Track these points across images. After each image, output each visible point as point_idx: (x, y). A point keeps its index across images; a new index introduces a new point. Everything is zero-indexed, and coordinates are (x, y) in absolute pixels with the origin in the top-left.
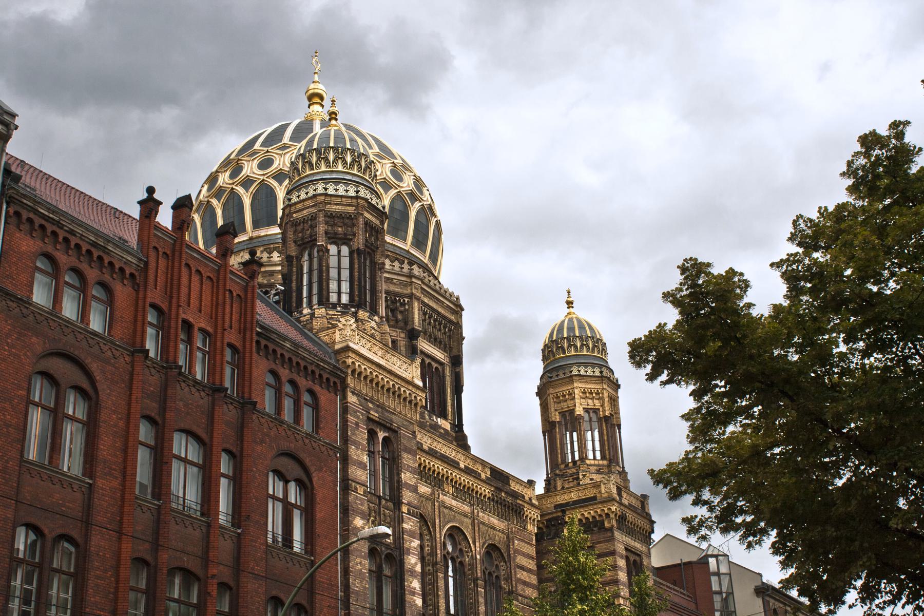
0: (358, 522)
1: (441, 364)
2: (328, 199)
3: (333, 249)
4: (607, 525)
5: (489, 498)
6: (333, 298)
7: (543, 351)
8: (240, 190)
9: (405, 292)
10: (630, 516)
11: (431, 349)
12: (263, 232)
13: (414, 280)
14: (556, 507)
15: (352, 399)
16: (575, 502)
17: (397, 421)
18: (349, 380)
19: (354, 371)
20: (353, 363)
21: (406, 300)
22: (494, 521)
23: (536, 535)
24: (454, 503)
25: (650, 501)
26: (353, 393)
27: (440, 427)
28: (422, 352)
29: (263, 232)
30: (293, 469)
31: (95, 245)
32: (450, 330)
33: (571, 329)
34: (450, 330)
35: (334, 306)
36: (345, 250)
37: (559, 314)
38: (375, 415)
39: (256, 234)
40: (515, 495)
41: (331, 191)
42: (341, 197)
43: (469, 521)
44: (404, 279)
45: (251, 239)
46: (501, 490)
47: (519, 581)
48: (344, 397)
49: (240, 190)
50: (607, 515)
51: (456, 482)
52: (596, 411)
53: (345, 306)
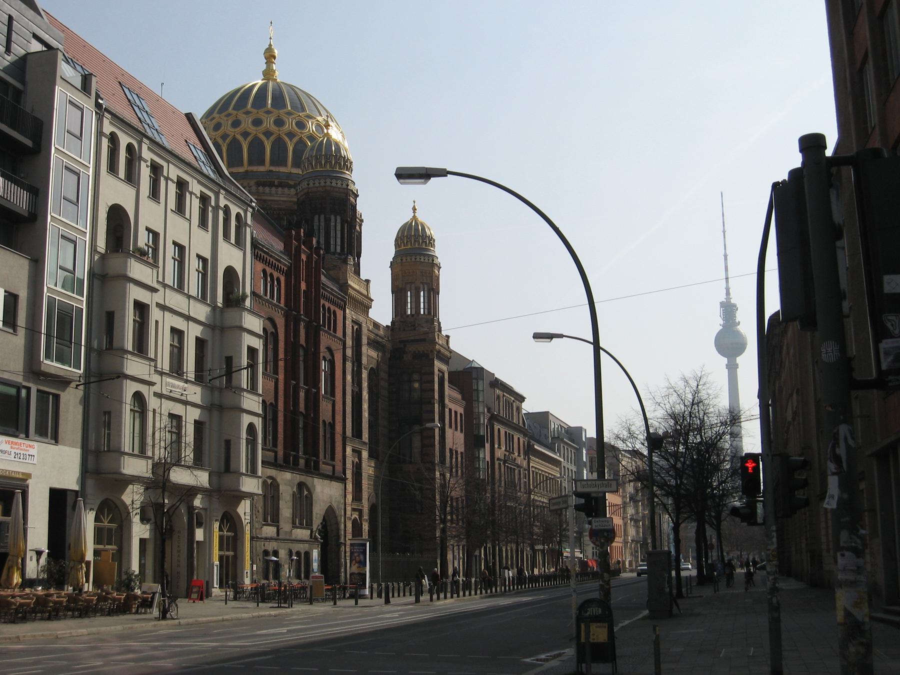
3: (333, 217)
4: (431, 357)
6: (332, 249)
7: (396, 240)
8: (241, 139)
10: (442, 350)
12: (255, 168)
14: (400, 342)
16: (413, 341)
25: (451, 340)
29: (255, 168)
30: (328, 357)
31: (277, 260)
33: (417, 229)
35: (334, 254)
36: (339, 218)
37: (407, 217)
39: (250, 168)
41: (334, 184)
45: (247, 172)
48: (345, 311)
49: (241, 139)
50: (432, 351)
52: (427, 283)
53: (339, 254)
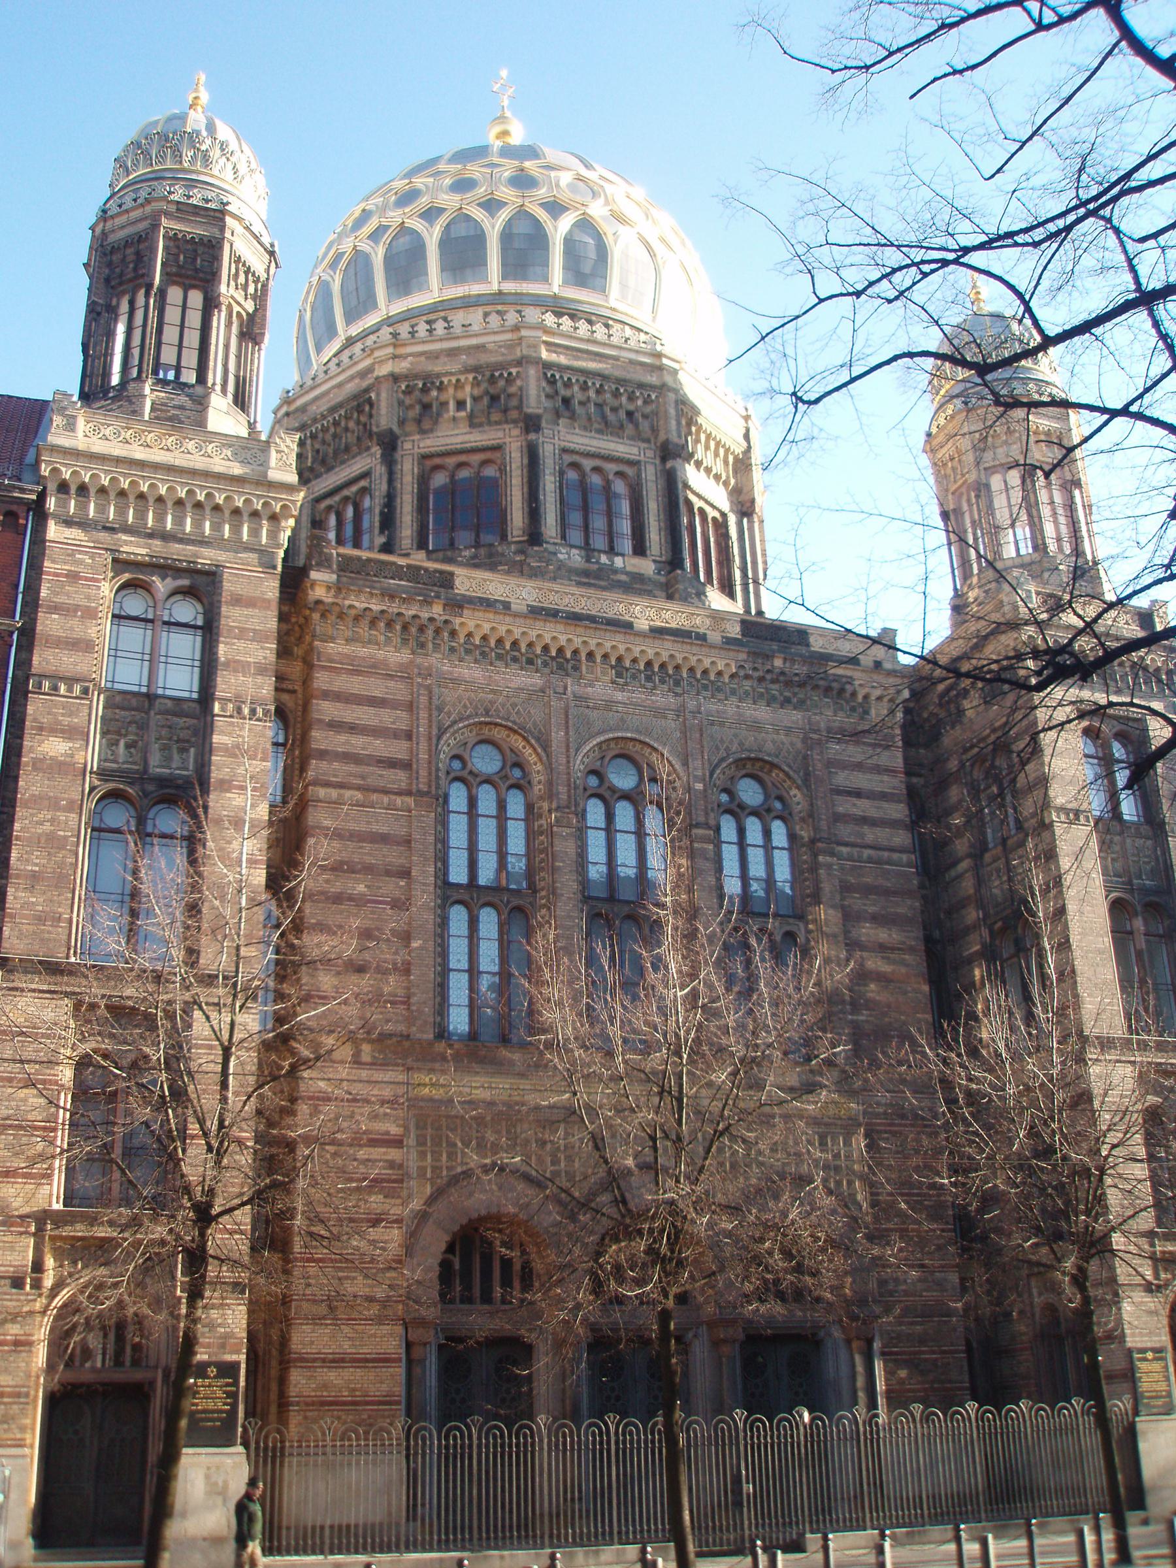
0: (55, 747)
1: (631, 463)
2: (109, 224)
5: (732, 676)
9: (509, 358)
11: (595, 443)
13: (524, 333)
15: (53, 531)
17: (206, 557)
18: (51, 503)
19: (63, 487)
20: (55, 471)
21: (514, 371)
22: (761, 712)
23: (904, 727)
24: (619, 696)
26: (68, 523)
27: (616, 571)
28: (565, 451)
32: (647, 401)
34: (647, 401)
38: (135, 548)
40: (825, 658)
42: (127, 211)
43: (671, 724)
44: (508, 336)
46: (768, 657)
47: (838, 818)
51: (620, 659)
